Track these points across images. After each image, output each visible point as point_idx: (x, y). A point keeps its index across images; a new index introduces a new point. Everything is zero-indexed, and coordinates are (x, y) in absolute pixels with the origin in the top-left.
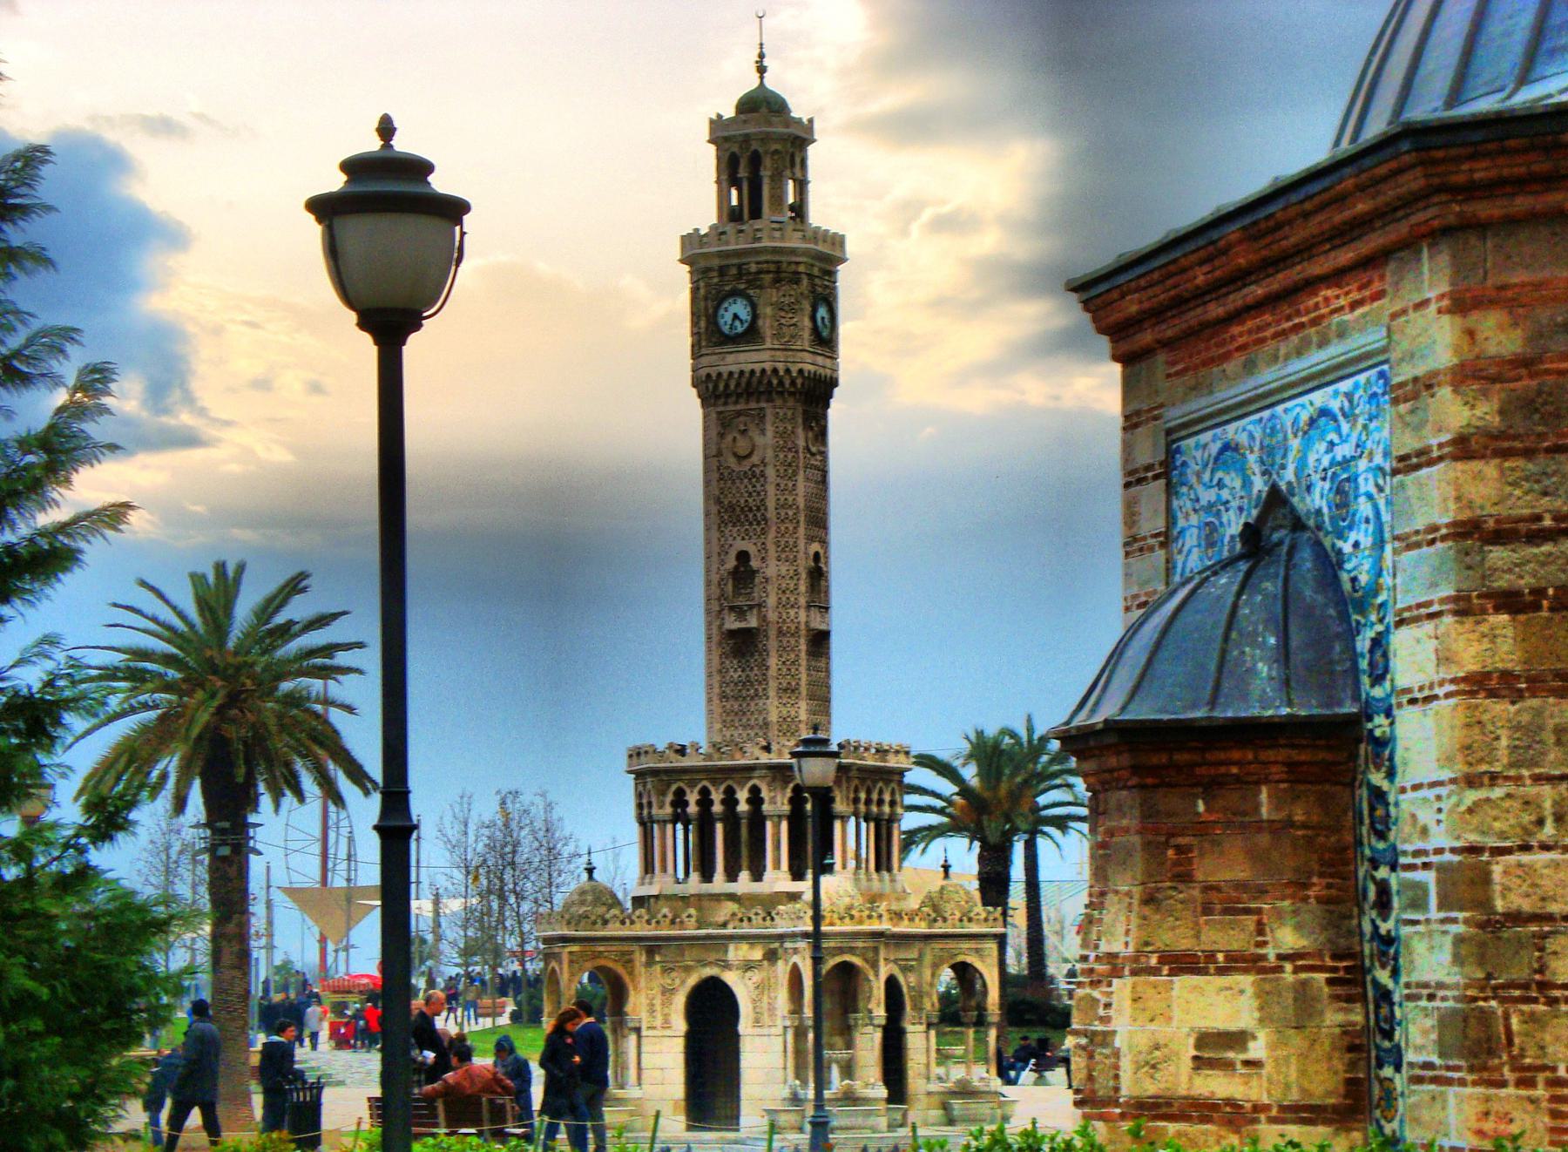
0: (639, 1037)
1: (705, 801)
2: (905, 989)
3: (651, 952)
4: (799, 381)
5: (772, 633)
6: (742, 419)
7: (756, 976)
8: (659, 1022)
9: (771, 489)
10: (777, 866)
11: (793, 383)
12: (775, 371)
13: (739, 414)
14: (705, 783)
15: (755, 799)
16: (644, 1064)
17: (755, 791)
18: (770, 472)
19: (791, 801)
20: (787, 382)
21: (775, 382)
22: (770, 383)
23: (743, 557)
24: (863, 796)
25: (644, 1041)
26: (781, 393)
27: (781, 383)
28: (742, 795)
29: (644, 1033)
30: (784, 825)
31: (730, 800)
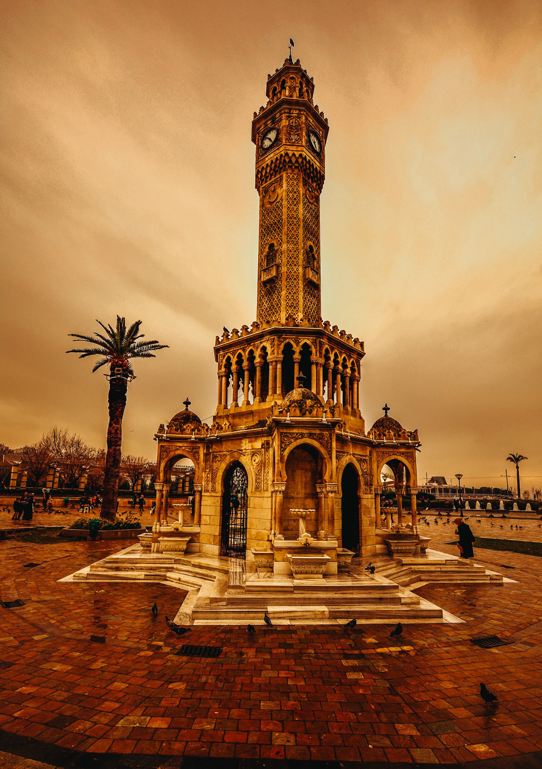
0: (201, 496)
1: (240, 361)
2: (360, 473)
3: (208, 448)
4: (300, 160)
5: (284, 277)
6: (273, 186)
7: (258, 459)
8: (210, 488)
9: (285, 210)
10: (275, 392)
11: (297, 161)
12: (287, 154)
13: (272, 184)
14: (240, 351)
15: (264, 355)
16: (202, 513)
17: (264, 349)
18: (285, 203)
19: (283, 352)
20: (294, 160)
21: (287, 160)
22: (285, 160)
23: (272, 246)
24: (332, 357)
25: (203, 498)
26: (290, 167)
27: (290, 161)
28: (257, 353)
29: (203, 494)
30: (279, 366)
31: (251, 357)
